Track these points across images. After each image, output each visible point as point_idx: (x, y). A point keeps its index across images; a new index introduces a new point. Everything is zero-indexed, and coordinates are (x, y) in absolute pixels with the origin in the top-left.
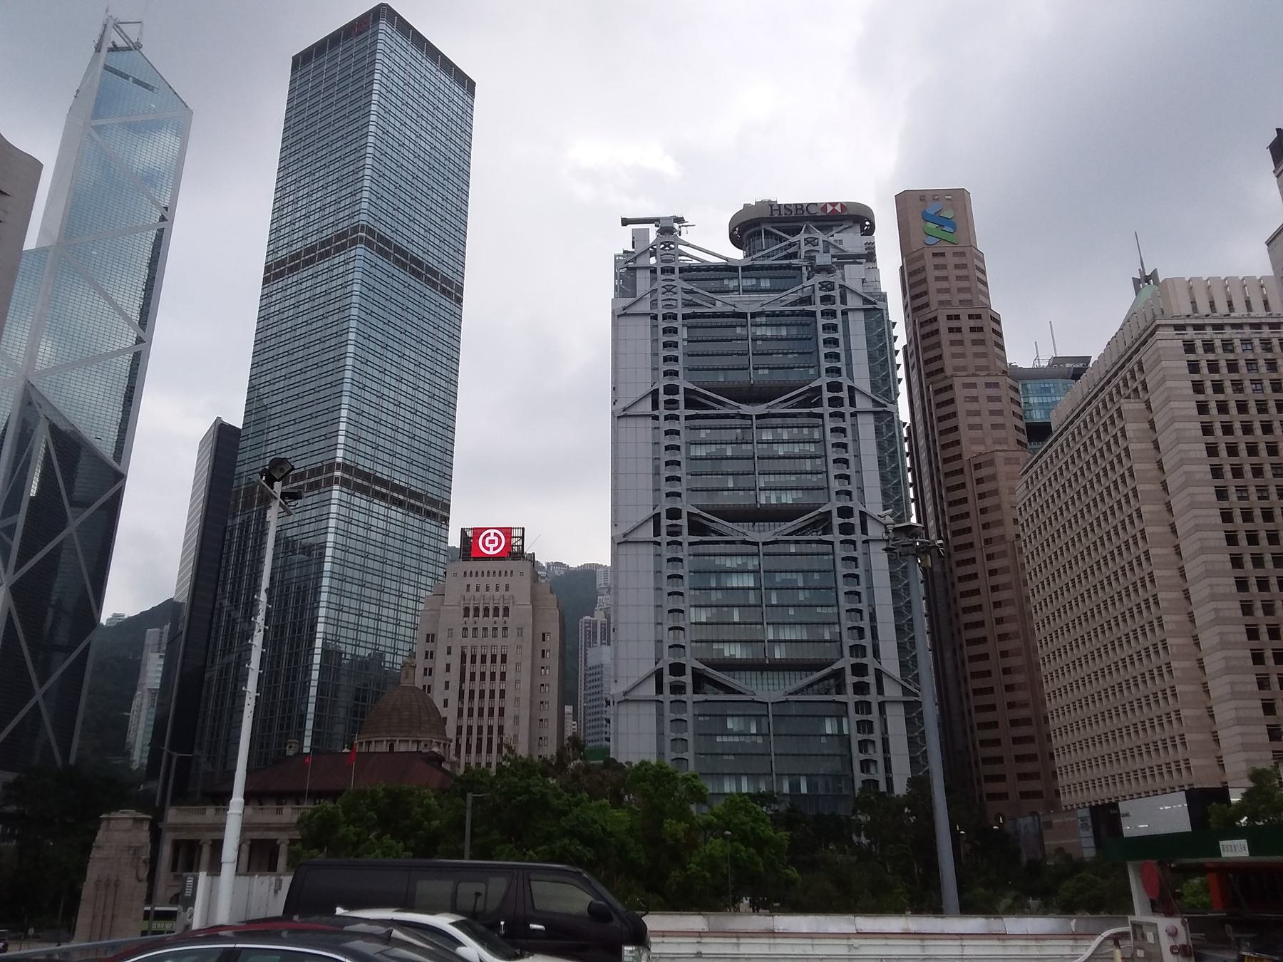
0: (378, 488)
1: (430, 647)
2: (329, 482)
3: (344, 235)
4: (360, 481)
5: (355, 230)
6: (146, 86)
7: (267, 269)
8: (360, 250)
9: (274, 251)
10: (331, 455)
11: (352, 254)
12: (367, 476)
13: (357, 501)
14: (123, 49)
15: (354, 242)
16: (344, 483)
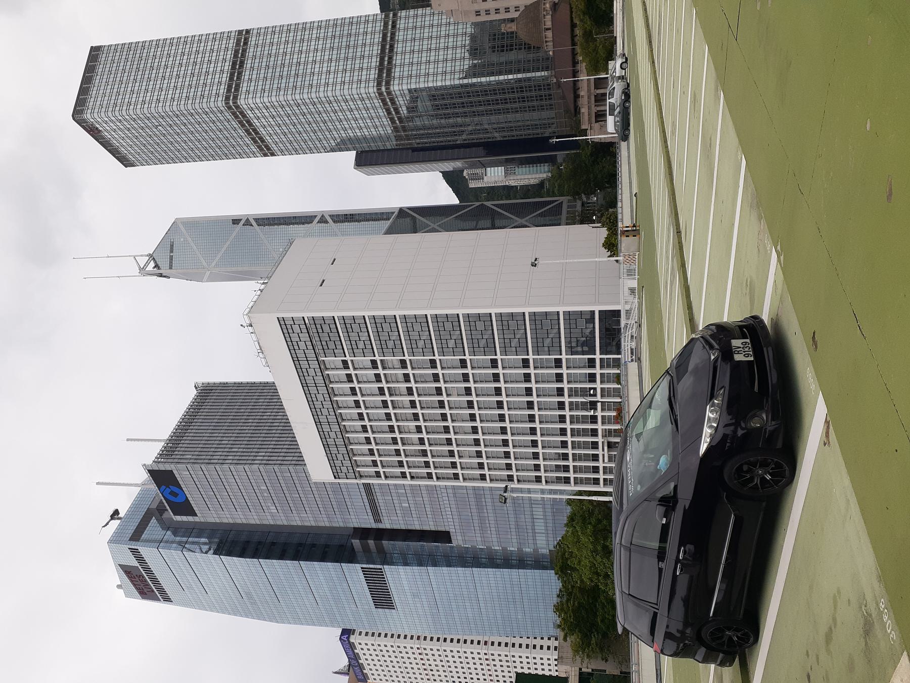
0: (386, 63)
1: (483, 13)
2: (389, 93)
3: (234, 114)
4: (385, 75)
5: (230, 108)
6: (172, 246)
7: (265, 155)
8: (241, 102)
9: (254, 153)
10: (373, 95)
11: (245, 106)
12: (381, 71)
13: (397, 74)
14: (155, 262)
15: (237, 107)
16: (388, 84)
